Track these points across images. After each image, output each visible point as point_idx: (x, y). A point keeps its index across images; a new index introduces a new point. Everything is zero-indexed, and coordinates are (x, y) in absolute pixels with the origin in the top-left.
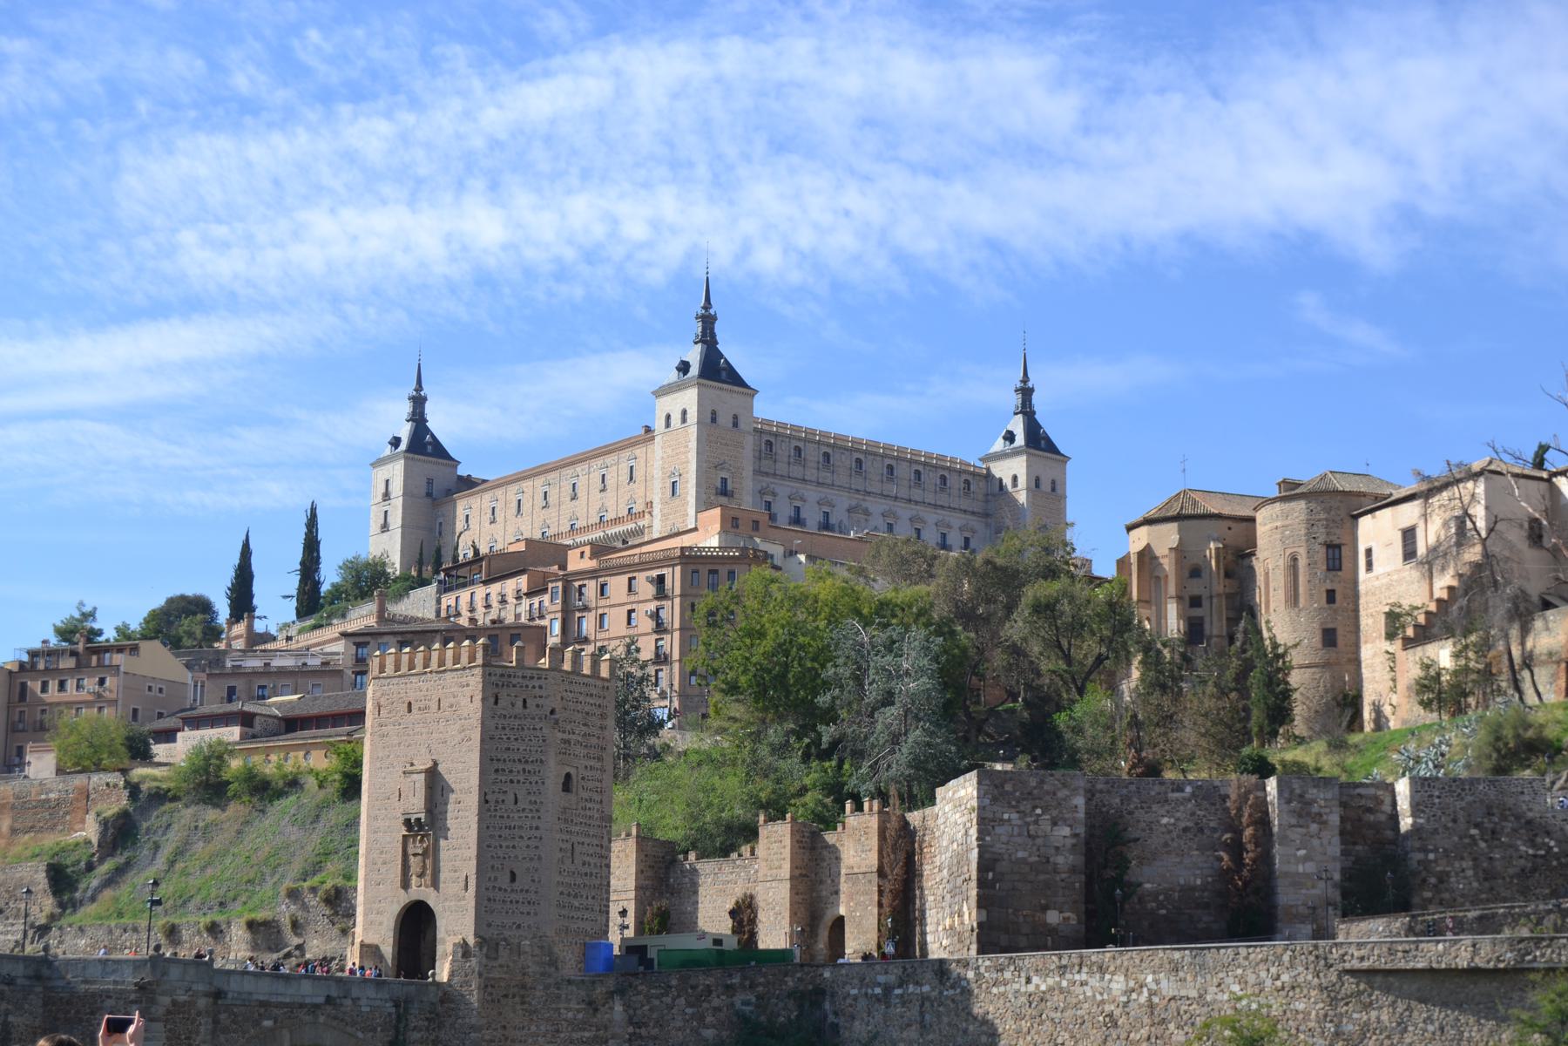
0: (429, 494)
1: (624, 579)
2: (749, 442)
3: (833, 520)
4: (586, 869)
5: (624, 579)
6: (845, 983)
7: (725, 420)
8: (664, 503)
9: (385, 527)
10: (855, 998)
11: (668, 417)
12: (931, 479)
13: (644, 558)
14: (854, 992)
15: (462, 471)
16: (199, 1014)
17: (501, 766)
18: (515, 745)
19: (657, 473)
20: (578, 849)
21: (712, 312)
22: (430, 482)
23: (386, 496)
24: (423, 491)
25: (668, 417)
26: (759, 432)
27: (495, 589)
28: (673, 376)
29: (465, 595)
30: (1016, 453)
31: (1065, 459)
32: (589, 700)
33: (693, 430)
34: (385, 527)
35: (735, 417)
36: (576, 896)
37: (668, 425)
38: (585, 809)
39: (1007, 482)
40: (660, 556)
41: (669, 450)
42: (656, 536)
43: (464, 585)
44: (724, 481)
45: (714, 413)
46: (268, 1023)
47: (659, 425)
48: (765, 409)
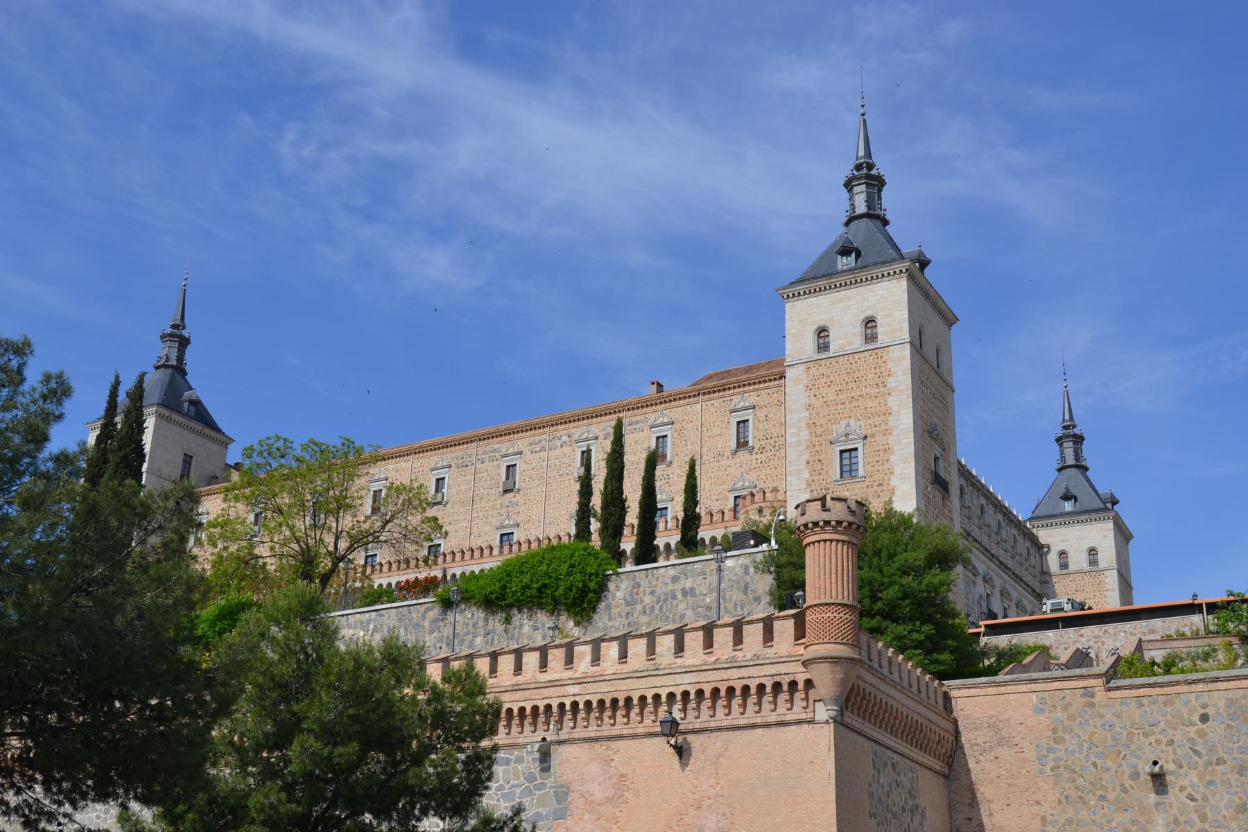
7: (930, 351)
22: (188, 460)
37: (823, 347)
39: (1078, 560)
41: (831, 394)
47: (799, 344)
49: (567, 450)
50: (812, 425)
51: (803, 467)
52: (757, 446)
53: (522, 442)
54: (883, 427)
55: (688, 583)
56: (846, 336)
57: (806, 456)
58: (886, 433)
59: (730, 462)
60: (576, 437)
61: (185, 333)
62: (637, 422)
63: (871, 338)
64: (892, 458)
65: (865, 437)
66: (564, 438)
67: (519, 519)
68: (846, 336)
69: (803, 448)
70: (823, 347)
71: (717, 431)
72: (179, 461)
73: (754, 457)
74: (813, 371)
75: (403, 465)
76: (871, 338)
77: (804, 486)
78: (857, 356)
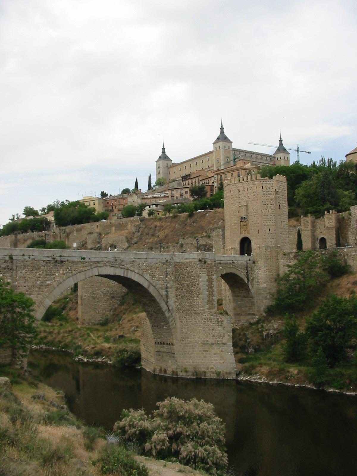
0: (167, 167)
1: (230, 174)
2: (232, 152)
4: (284, 228)
5: (230, 174)
6: (351, 252)
8: (216, 164)
10: (354, 255)
12: (264, 158)
13: (227, 171)
14: (353, 254)
15: (173, 162)
16: (213, 266)
17: (265, 203)
18: (268, 198)
19: (214, 159)
20: (283, 223)
21: (223, 127)
22: (167, 164)
29: (187, 182)
32: (283, 187)
35: (229, 147)
36: (283, 234)
38: (283, 213)
40: (230, 170)
42: (222, 169)
43: (187, 180)
46: (221, 268)
48: (235, 146)
50: (215, 158)
56: (218, 149)
72: (166, 164)
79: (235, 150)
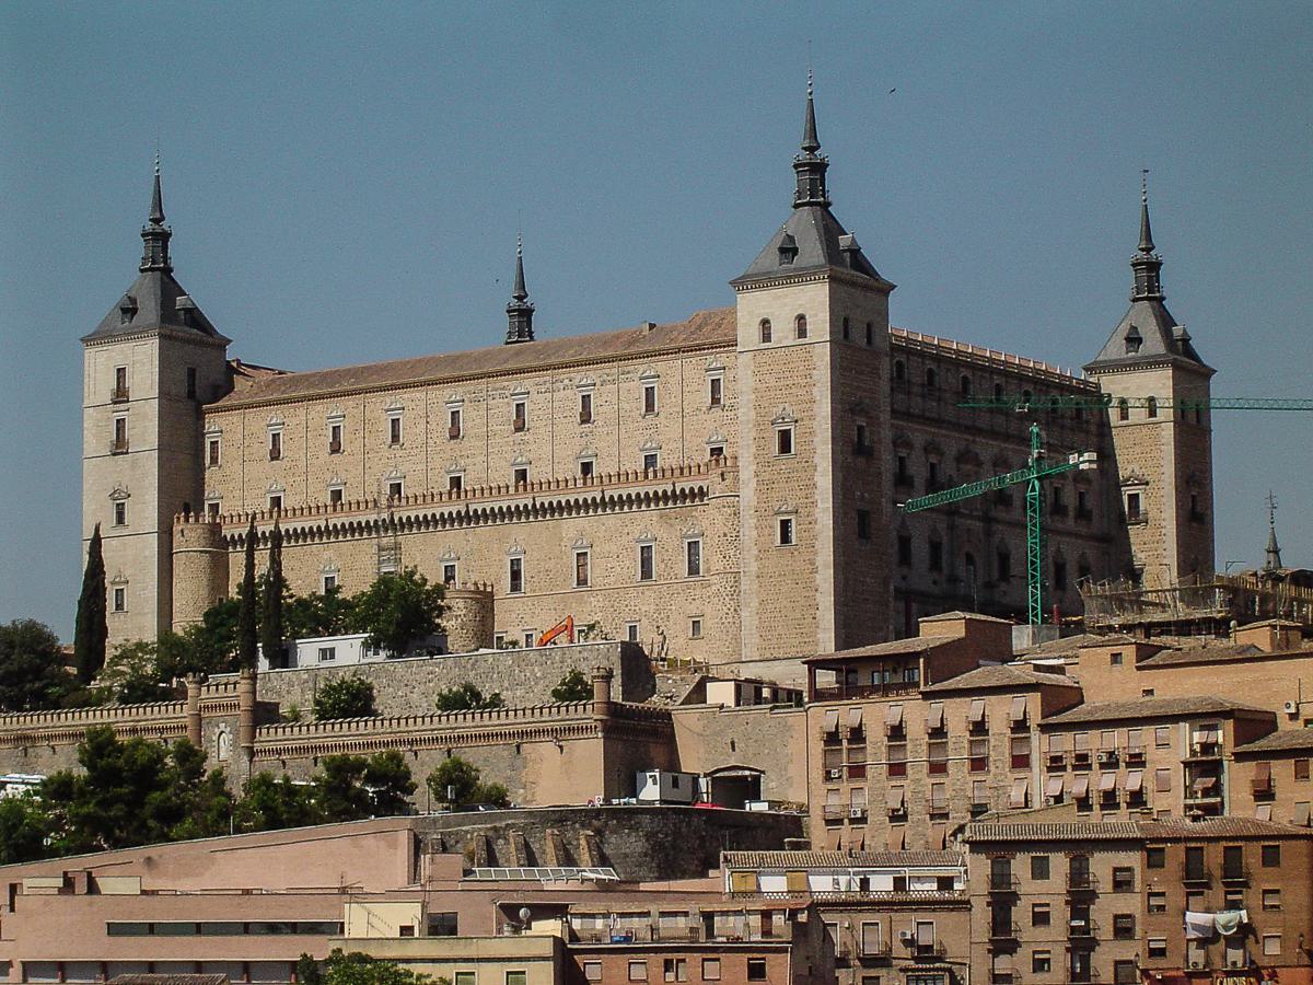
0: (191, 394)
2: (886, 368)
3: (942, 478)
8: (762, 463)
9: (120, 446)
11: (765, 323)
15: (231, 355)
22: (192, 373)
23: (121, 395)
24: (184, 390)
25: (765, 323)
26: (895, 349)
27: (959, 714)
28: (772, 261)
30: (1153, 363)
31: (885, 289)
33: (823, 356)
34: (120, 446)
37: (767, 337)
44: (860, 429)
45: (846, 321)
47: (748, 334)
49: (569, 392)
51: (751, 442)
52: (727, 404)
53: (527, 382)
54: (810, 413)
55: (585, 654)
56: (783, 331)
57: (754, 434)
58: (812, 418)
59: (705, 417)
60: (576, 382)
61: (165, 225)
62: (629, 373)
63: (802, 333)
64: (815, 439)
65: (796, 421)
66: (567, 381)
67: (531, 456)
68: (783, 331)
69: (751, 426)
70: (767, 337)
71: (695, 387)
73: (725, 413)
74: (758, 358)
75: (418, 395)
76: (802, 333)
77: (752, 459)
78: (791, 349)
79: (907, 352)
